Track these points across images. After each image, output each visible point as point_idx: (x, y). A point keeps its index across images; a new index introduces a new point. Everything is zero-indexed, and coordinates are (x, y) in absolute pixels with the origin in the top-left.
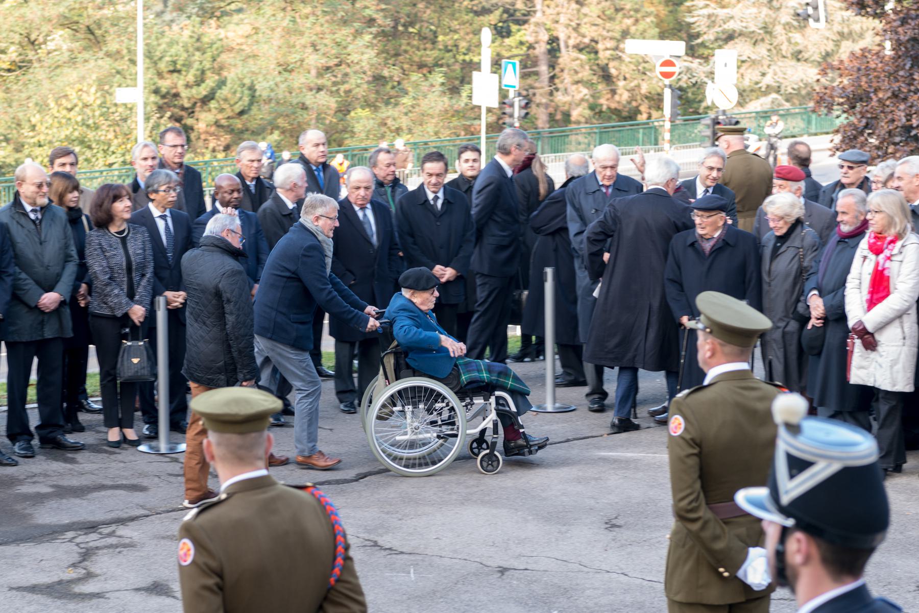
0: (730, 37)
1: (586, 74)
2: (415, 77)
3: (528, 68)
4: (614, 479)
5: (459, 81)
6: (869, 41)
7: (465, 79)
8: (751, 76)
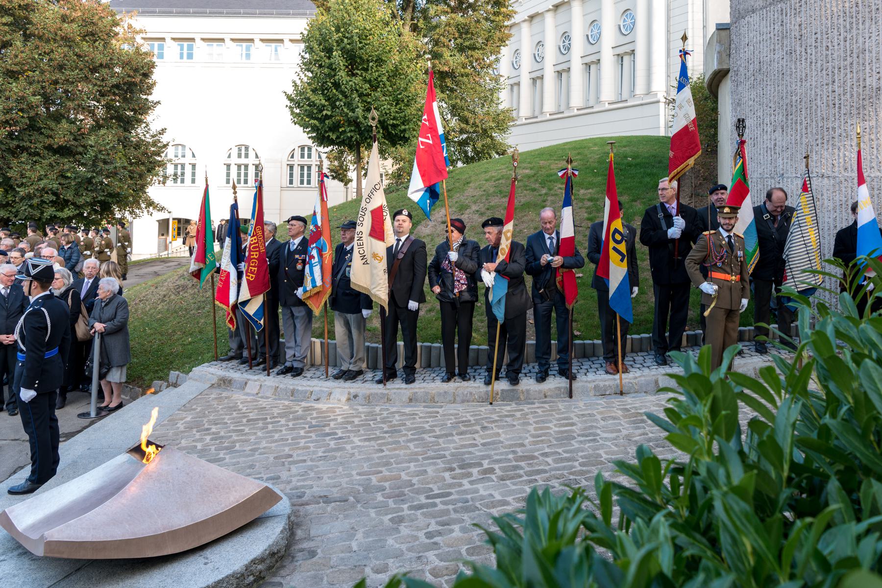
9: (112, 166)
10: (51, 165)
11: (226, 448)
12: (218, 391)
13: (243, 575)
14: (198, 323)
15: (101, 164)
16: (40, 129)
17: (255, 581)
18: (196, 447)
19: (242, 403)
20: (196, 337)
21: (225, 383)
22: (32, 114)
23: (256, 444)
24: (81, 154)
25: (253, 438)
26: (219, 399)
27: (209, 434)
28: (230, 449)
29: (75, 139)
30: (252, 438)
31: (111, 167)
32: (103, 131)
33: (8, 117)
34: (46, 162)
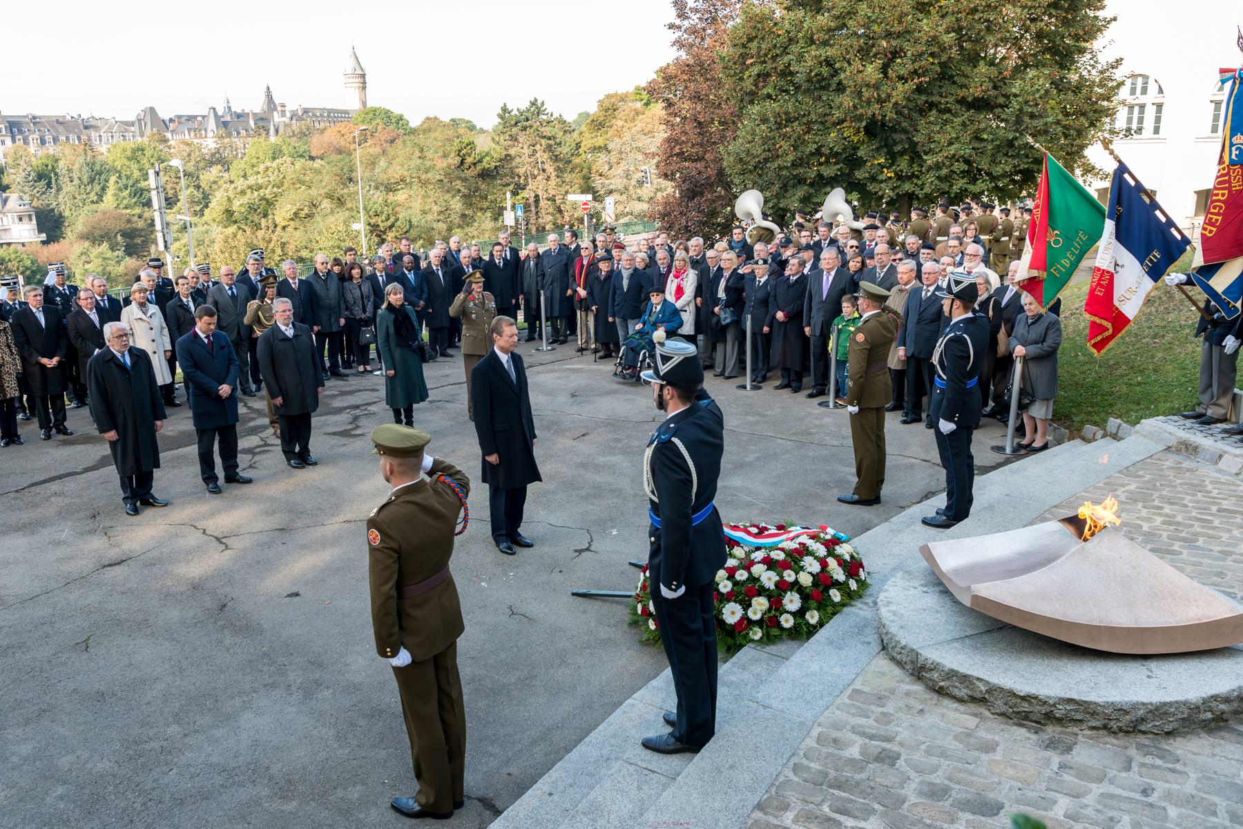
0: (611, 192)
1: (551, 210)
2: (479, 214)
3: (526, 208)
4: (573, 377)
5: (498, 213)
6: (670, 190)
7: (501, 214)
8: (621, 208)
9: (1042, 121)
10: (964, 124)
11: (1184, 540)
12: (1177, 458)
13: (1198, 707)
14: (1153, 357)
15: (1027, 119)
16: (952, 77)
17: (1213, 719)
18: (1141, 527)
19: (1211, 482)
20: (1149, 376)
21: (1189, 449)
22: (944, 58)
23: (1229, 545)
24: (1002, 106)
25: (1225, 536)
26: (1178, 469)
27: (1160, 514)
28: (1190, 542)
29: (995, 88)
30: (1225, 536)
31: (1038, 123)
32: (1031, 73)
33: (917, 65)
34: (958, 120)
